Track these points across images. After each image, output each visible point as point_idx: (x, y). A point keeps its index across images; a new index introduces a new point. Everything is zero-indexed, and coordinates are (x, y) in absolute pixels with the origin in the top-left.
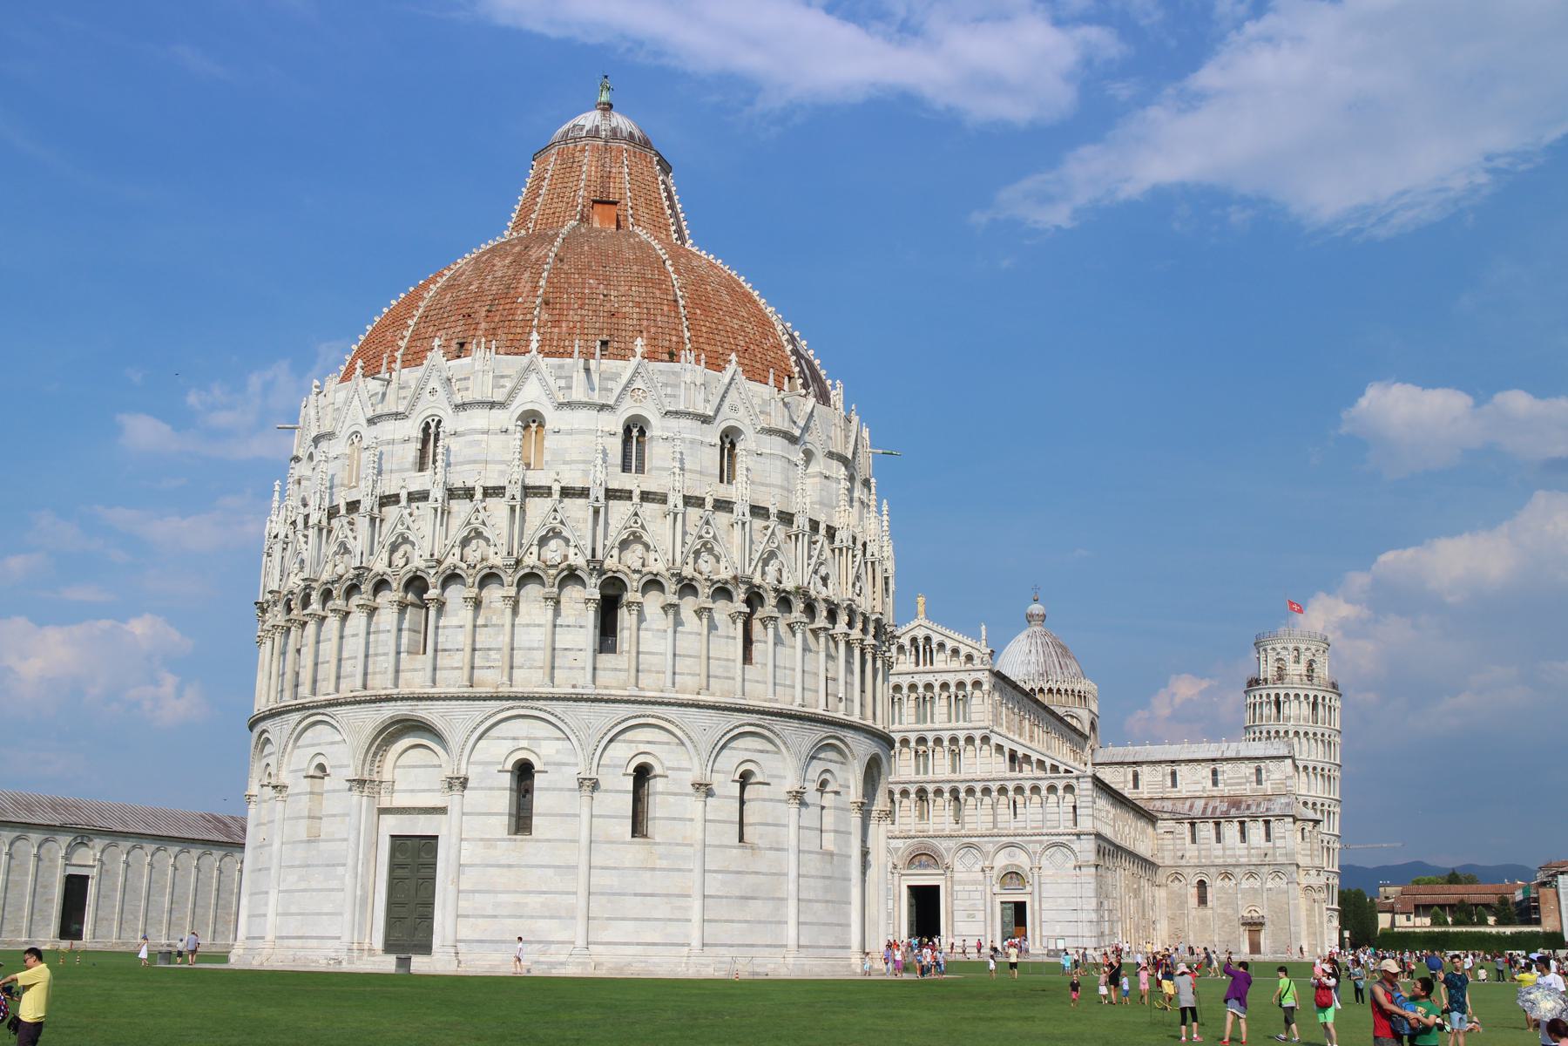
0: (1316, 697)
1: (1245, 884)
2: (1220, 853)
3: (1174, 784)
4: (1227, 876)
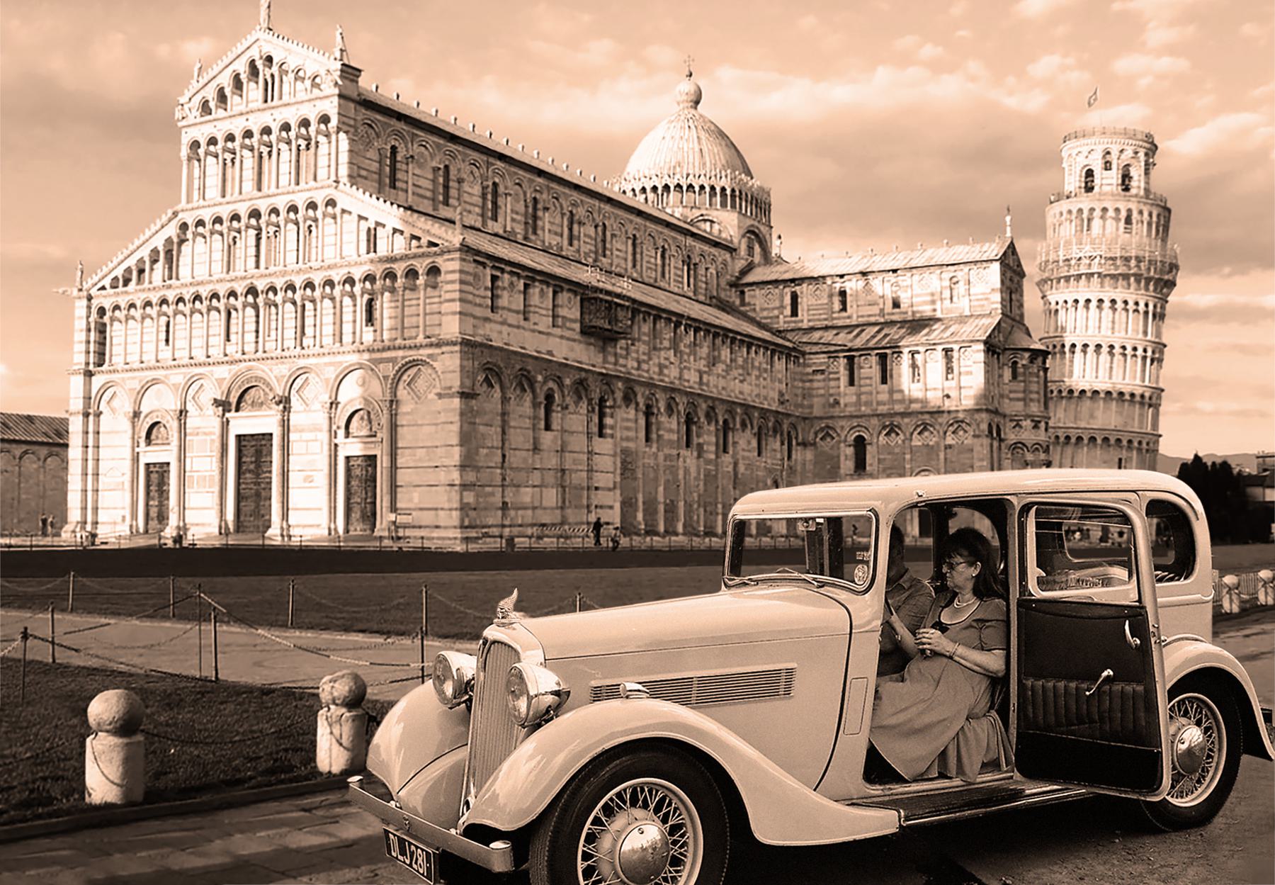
0: (1129, 211)
1: (917, 441)
2: (884, 397)
3: (844, 309)
4: (892, 430)
